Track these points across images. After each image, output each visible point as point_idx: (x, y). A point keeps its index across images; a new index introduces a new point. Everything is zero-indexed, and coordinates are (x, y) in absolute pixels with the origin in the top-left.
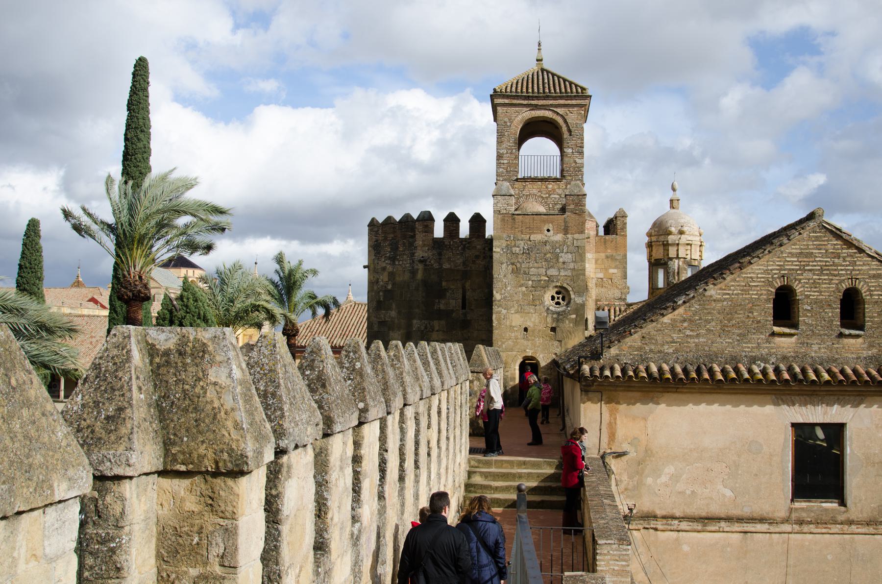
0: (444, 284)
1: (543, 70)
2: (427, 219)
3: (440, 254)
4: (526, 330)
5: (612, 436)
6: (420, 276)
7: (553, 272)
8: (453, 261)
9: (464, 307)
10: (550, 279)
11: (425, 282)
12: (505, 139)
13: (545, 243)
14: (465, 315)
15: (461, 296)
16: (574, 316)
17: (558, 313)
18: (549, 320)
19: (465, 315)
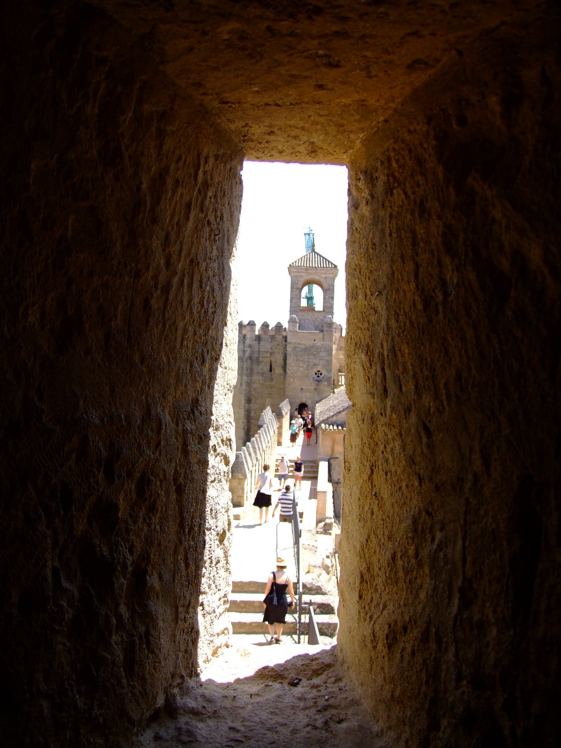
0: (261, 359)
1: (315, 253)
2: (252, 324)
3: (259, 343)
4: (302, 389)
5: (333, 451)
6: (247, 354)
7: (317, 361)
8: (266, 346)
9: (271, 370)
10: (315, 365)
11: (250, 358)
12: (294, 290)
13: (313, 347)
14: (271, 375)
15: (269, 366)
16: (326, 383)
17: (318, 381)
18: (314, 384)
19: (271, 375)
